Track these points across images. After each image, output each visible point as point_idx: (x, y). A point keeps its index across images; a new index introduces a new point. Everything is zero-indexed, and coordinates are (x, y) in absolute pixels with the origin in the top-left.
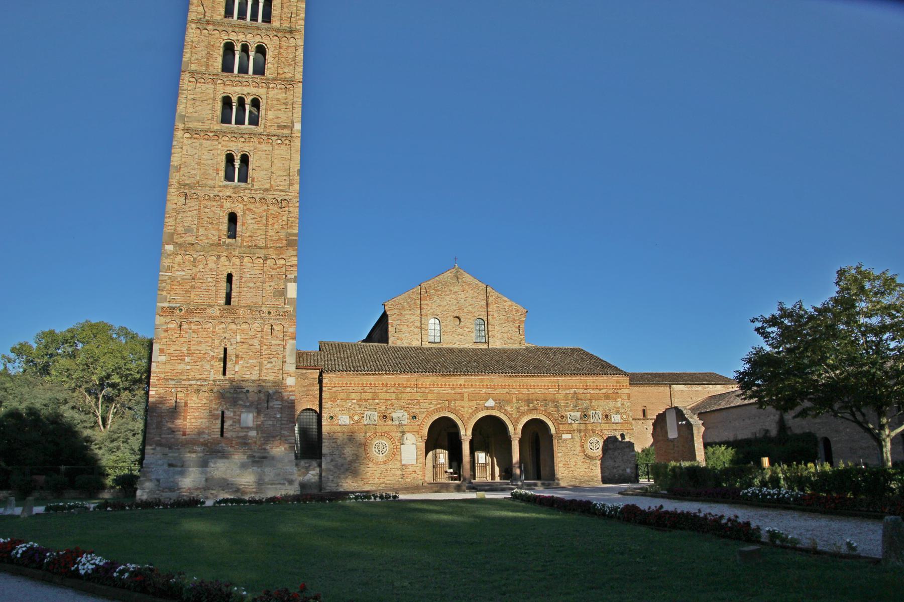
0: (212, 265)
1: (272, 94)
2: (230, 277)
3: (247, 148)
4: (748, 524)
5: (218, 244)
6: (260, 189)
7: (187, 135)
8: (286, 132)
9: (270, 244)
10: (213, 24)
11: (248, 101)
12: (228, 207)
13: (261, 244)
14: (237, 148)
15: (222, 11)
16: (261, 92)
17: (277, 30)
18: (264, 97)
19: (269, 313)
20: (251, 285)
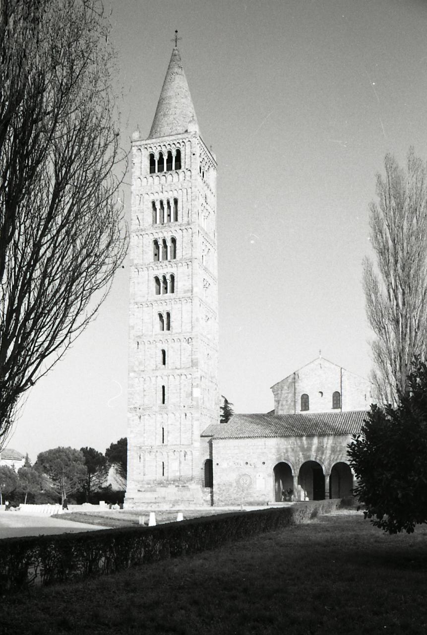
0: (153, 382)
1: (180, 270)
2: (163, 387)
3: (168, 309)
4: (421, 524)
5: (156, 370)
6: (177, 333)
7: (136, 306)
8: (189, 294)
9: (183, 366)
10: (145, 230)
11: (168, 277)
12: (161, 346)
13: (179, 367)
14: (163, 311)
15: (150, 220)
16: (173, 270)
17: (180, 225)
18: (175, 273)
19: (184, 407)
20: (175, 391)
